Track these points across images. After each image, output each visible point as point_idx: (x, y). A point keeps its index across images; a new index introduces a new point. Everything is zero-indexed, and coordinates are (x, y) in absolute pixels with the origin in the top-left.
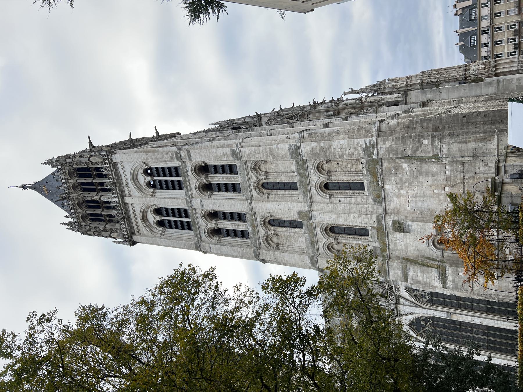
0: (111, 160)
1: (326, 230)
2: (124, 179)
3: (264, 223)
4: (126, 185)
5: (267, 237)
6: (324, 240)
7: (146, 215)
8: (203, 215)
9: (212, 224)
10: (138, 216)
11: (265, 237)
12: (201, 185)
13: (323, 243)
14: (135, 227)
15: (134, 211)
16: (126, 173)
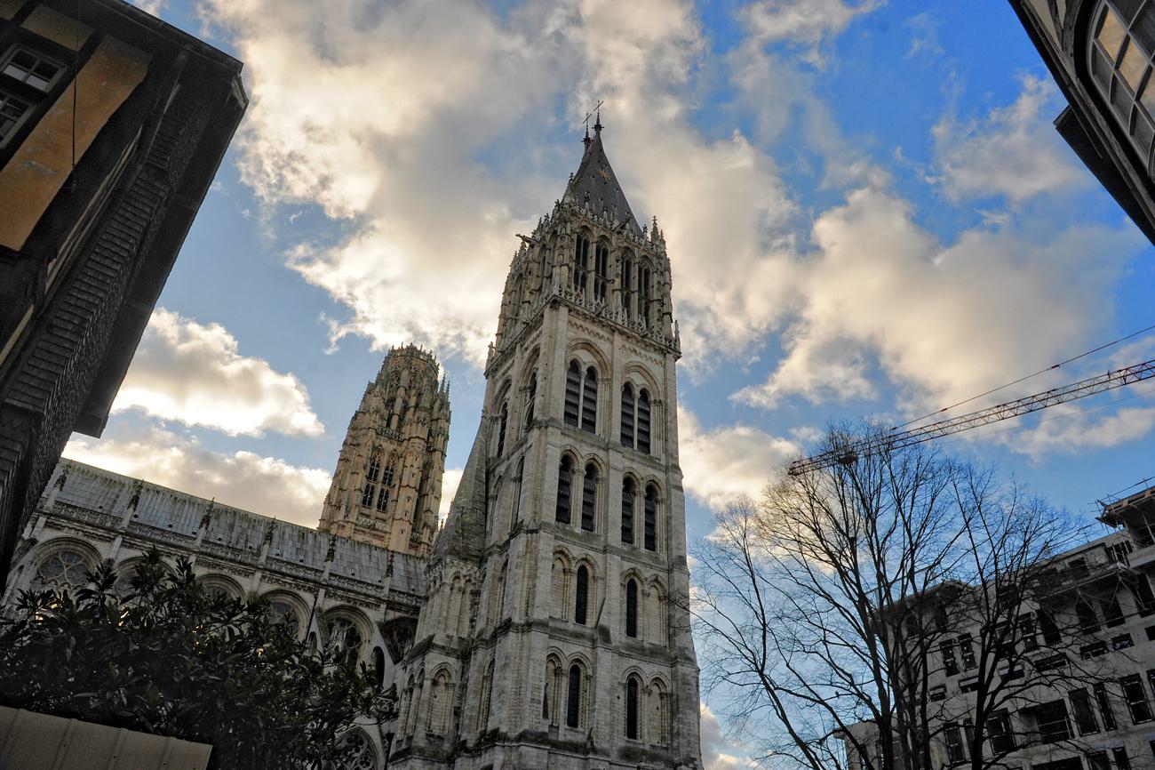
0: (669, 353)
1: (578, 660)
2: (643, 352)
3: (585, 559)
4: (635, 351)
5: (566, 556)
6: (567, 654)
7: (589, 351)
8: (596, 458)
9: (580, 465)
10: (593, 340)
11: (567, 552)
12: (634, 478)
13: (561, 648)
14: (579, 322)
15: (601, 337)
16: (649, 362)
